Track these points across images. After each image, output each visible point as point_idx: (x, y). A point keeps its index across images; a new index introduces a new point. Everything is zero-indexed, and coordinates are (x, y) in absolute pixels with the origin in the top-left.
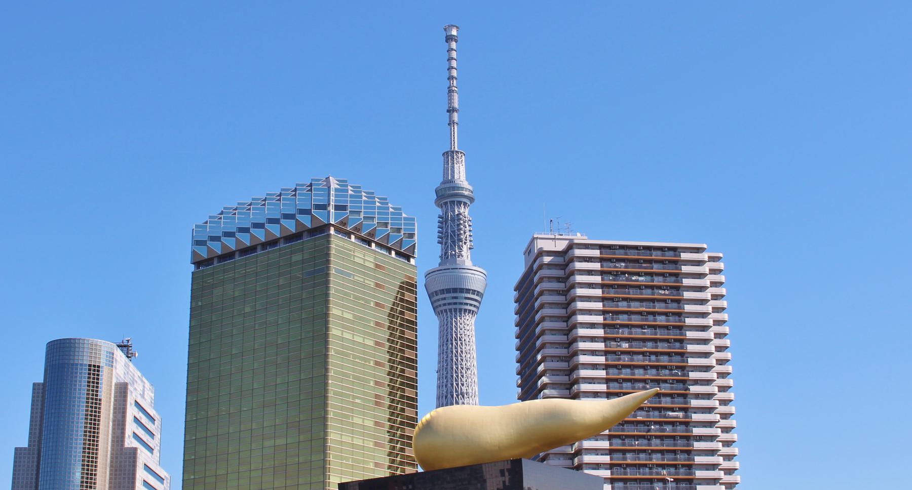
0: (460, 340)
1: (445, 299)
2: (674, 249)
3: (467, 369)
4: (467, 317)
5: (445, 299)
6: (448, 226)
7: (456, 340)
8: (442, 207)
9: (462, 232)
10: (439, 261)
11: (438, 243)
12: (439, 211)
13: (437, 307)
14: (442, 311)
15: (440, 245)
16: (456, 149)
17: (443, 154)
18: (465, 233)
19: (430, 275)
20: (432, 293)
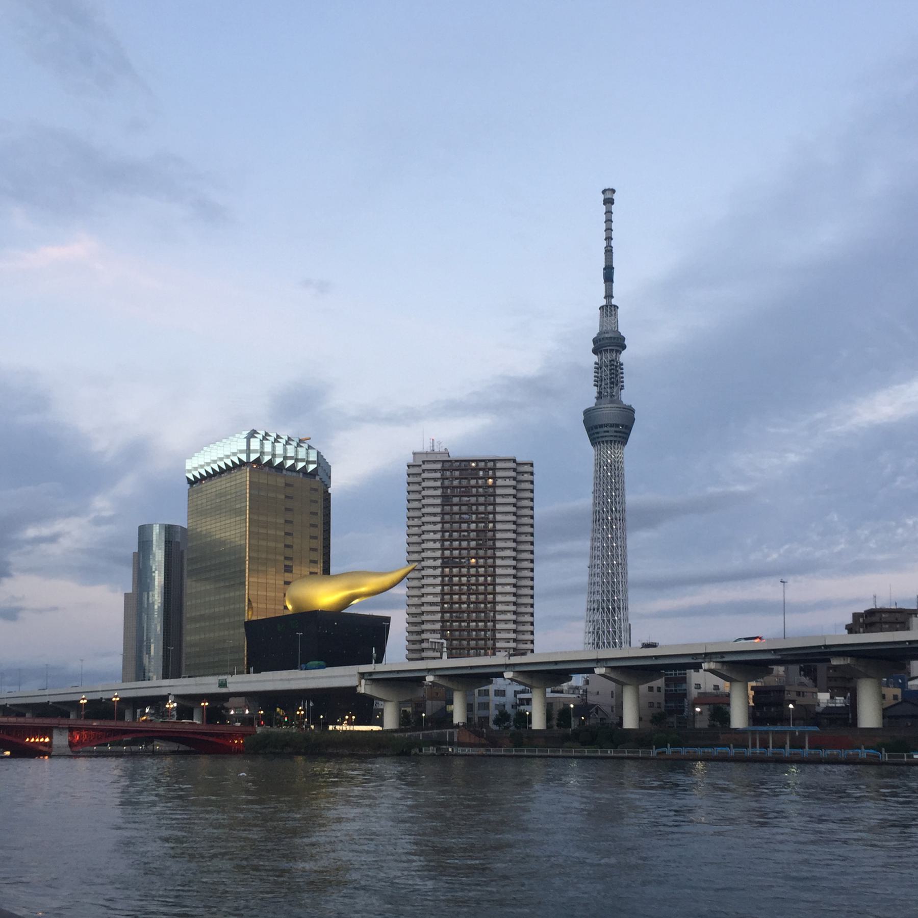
1: (598, 433)
2: (494, 461)
5: (598, 433)
10: (595, 400)
11: (595, 385)
12: (595, 358)
13: (594, 439)
15: (596, 387)
18: (617, 376)
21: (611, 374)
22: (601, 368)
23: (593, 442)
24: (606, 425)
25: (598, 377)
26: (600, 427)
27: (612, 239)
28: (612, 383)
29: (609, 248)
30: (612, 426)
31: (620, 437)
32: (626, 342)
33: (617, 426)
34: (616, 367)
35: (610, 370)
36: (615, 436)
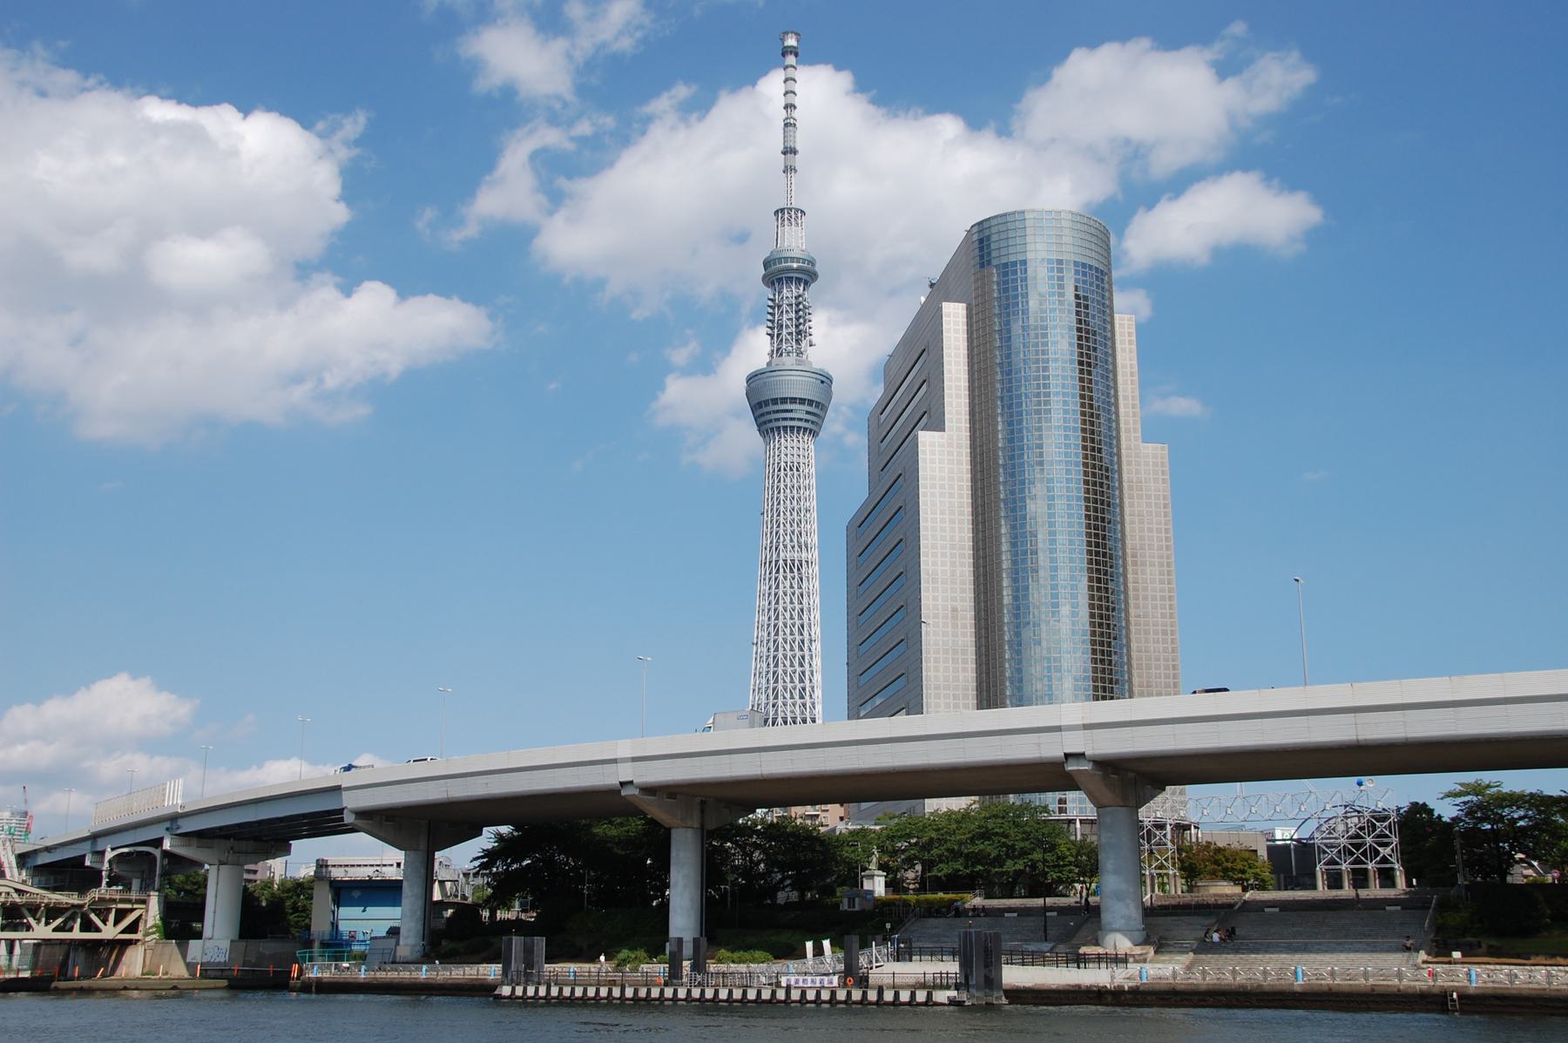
0: (798, 470)
3: (807, 511)
4: (806, 438)
6: (782, 312)
7: (791, 470)
8: (773, 284)
9: (801, 321)
11: (768, 334)
12: (769, 293)
13: (765, 423)
14: (772, 429)
15: (769, 337)
16: (793, 206)
17: (776, 212)
18: (805, 321)
19: (756, 378)
20: (755, 406)
21: (797, 319)
22: (779, 307)
23: (764, 427)
24: (793, 400)
25: (772, 321)
26: (782, 403)
27: (795, 108)
28: (799, 333)
29: (792, 121)
30: (802, 401)
31: (813, 422)
32: (818, 269)
33: (810, 402)
34: (804, 306)
35: (797, 312)
36: (807, 421)
